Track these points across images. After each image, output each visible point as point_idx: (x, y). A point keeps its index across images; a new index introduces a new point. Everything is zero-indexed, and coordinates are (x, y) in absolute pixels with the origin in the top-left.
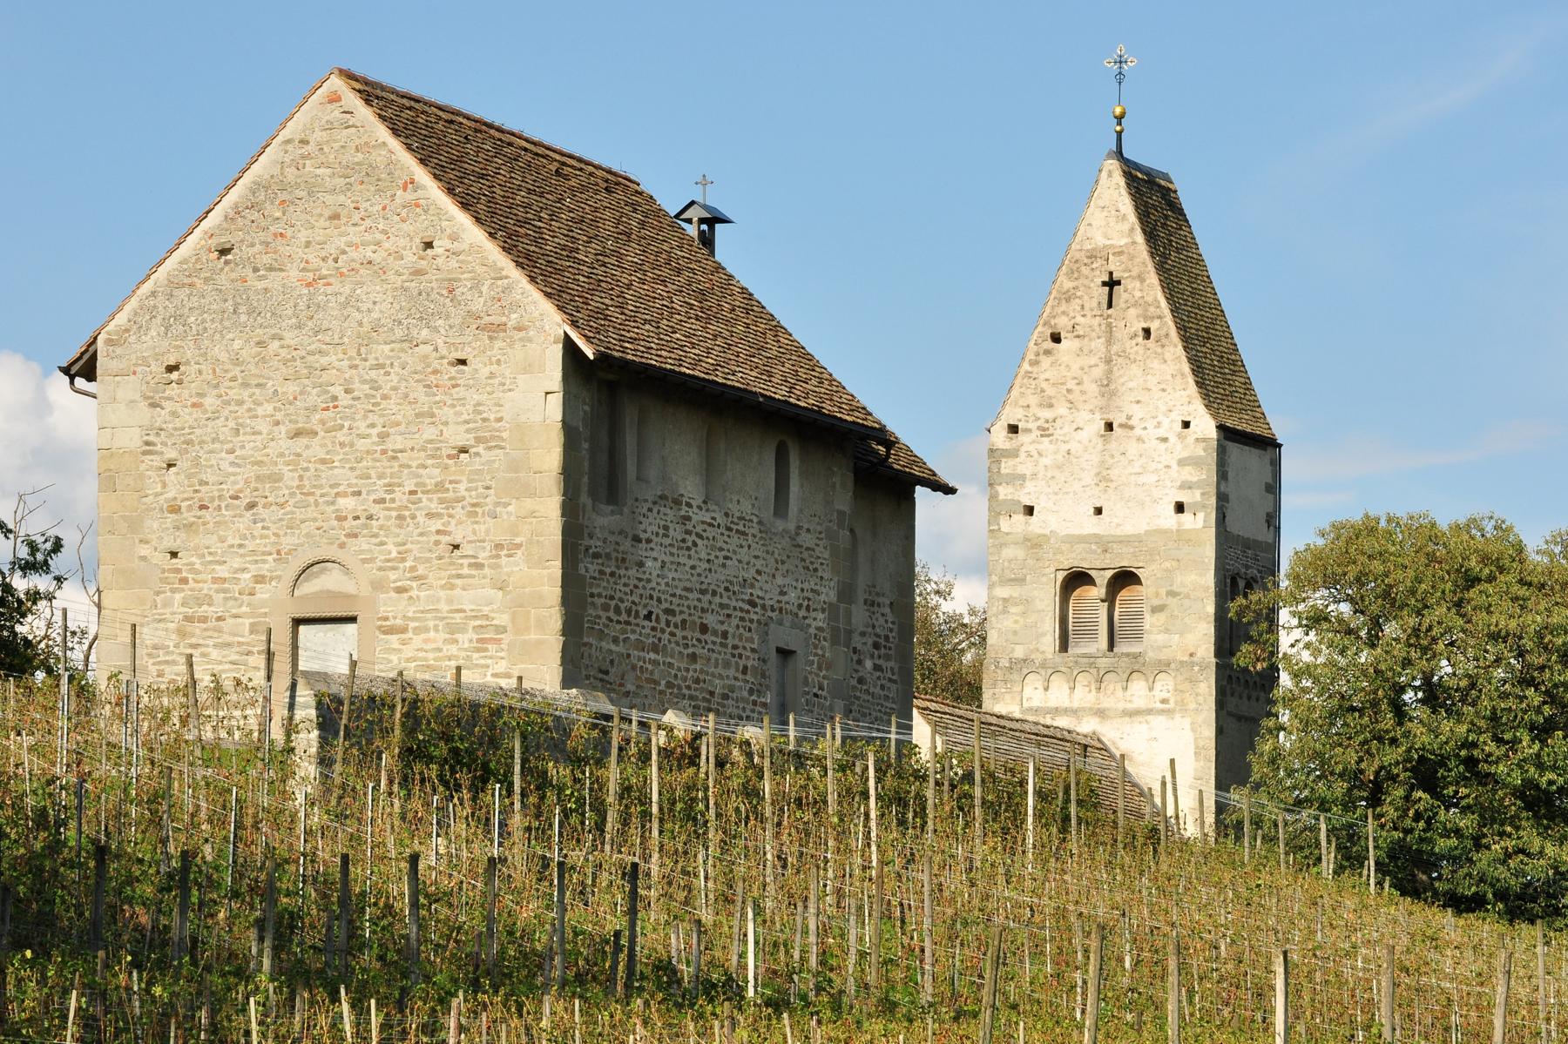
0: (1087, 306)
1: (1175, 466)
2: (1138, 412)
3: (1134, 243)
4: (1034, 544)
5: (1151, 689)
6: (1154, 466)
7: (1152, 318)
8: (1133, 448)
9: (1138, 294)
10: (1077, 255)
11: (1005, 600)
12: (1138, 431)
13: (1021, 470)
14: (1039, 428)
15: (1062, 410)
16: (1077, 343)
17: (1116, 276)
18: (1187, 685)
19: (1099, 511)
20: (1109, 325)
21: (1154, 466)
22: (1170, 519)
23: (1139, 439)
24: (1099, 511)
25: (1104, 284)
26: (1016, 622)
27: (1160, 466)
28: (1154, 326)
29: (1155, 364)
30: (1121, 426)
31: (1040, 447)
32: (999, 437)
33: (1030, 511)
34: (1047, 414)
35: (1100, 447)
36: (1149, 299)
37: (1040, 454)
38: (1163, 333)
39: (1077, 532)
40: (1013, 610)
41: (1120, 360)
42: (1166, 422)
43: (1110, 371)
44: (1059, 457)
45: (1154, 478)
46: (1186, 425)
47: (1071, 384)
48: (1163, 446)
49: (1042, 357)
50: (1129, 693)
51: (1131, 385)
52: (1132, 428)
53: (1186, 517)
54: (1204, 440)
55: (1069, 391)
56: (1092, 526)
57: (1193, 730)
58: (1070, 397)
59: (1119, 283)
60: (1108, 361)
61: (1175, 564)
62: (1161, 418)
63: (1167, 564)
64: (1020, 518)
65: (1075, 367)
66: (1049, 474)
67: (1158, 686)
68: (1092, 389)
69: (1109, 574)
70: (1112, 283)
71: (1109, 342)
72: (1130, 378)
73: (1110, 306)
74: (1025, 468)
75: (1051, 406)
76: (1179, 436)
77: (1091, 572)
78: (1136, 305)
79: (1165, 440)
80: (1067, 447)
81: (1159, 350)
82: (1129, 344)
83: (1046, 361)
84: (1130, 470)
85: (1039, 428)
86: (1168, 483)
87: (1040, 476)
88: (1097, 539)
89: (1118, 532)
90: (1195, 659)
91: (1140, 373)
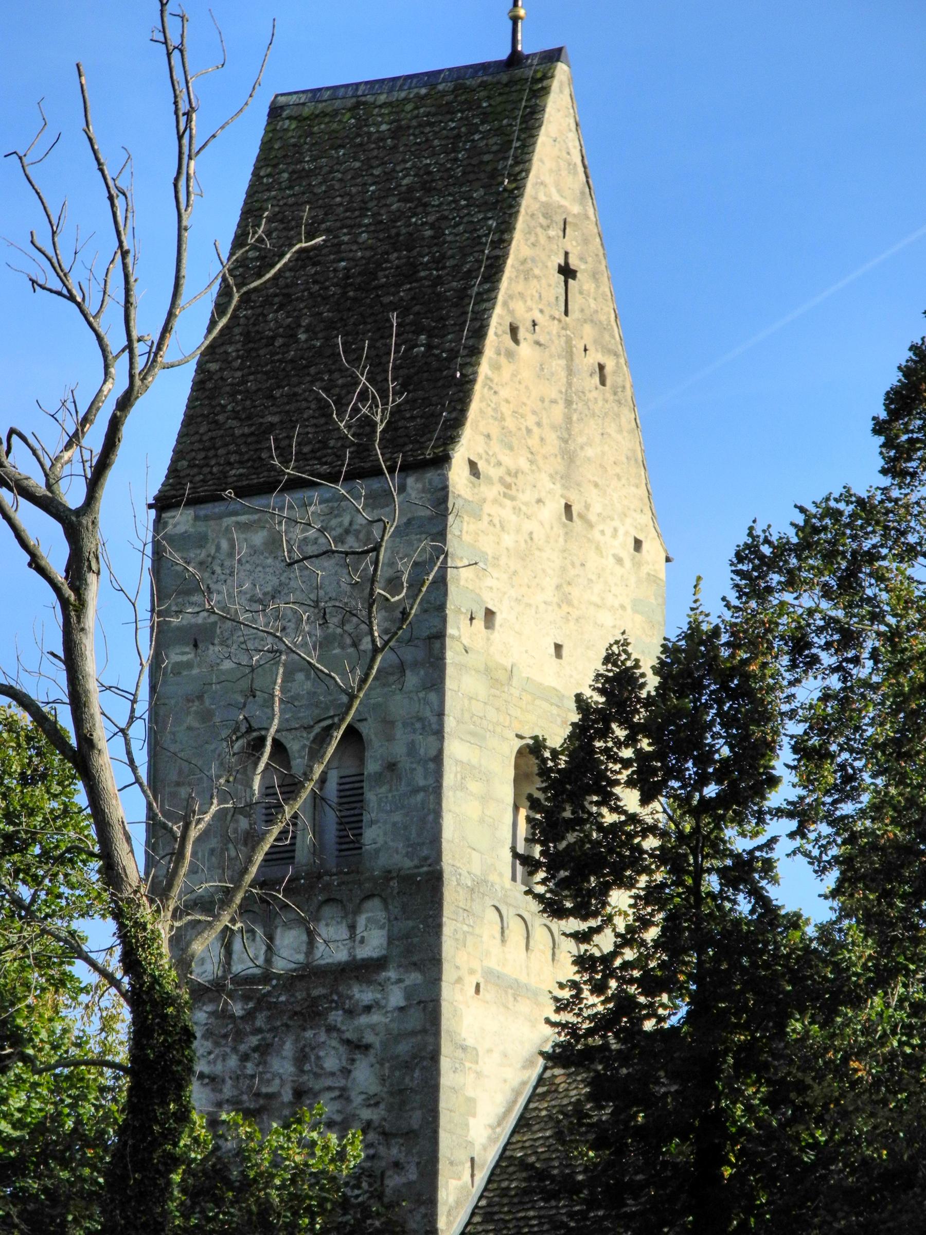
3: (587, 218)
17: (574, 262)
20: (569, 341)
29: (612, 429)
36: (603, 318)
60: (569, 403)
70: (567, 272)
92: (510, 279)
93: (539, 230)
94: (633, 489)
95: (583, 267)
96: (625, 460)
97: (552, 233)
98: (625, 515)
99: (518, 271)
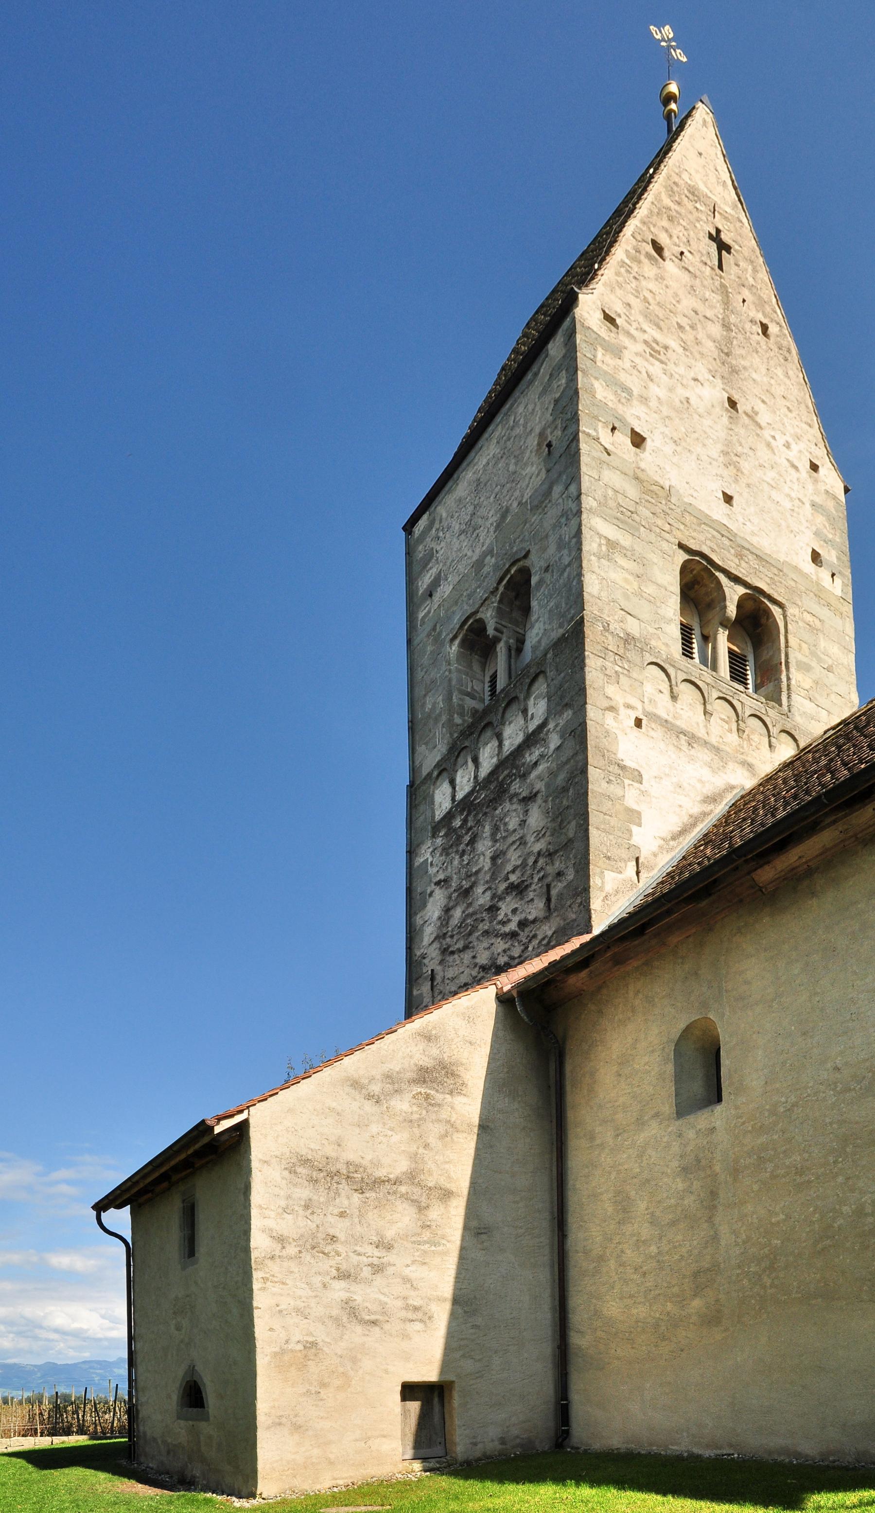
8: (763, 453)
11: (612, 545)
14: (646, 342)
17: (725, 237)
21: (787, 490)
26: (626, 580)
29: (779, 372)
31: (651, 369)
35: (725, 420)
40: (622, 561)
41: (740, 336)
47: (684, 322)
52: (761, 428)
55: (680, 327)
60: (726, 326)
64: (623, 440)
66: (665, 411)
71: (727, 303)
73: (720, 267)
82: (748, 326)
85: (646, 342)
95: (737, 247)
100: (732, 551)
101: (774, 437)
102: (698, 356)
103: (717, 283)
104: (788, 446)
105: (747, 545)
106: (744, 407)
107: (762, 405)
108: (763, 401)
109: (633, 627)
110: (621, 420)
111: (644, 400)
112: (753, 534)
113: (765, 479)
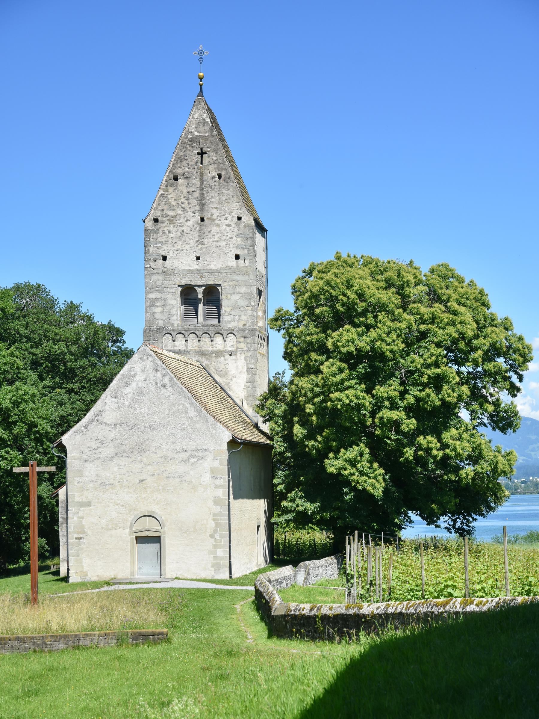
0: (190, 164)
1: (235, 238)
2: (216, 213)
4: (167, 273)
5: (225, 341)
6: (225, 237)
7: (222, 169)
8: (214, 230)
9: (215, 158)
10: (185, 140)
12: (217, 222)
13: (160, 239)
14: (169, 220)
15: (179, 212)
16: (186, 181)
18: (242, 339)
19: (198, 258)
20: (202, 174)
21: (225, 237)
22: (233, 262)
23: (218, 225)
24: (198, 258)
25: (198, 153)
27: (228, 238)
28: (223, 173)
30: (207, 219)
31: (169, 229)
32: (150, 224)
33: (164, 258)
34: (172, 213)
37: (169, 232)
38: (228, 176)
39: (187, 268)
42: (230, 217)
43: (202, 194)
44: (179, 234)
45: (224, 243)
46: (239, 219)
48: (228, 228)
49: (169, 187)
50: (214, 343)
51: (213, 200)
52: (214, 220)
53: (241, 261)
54: (249, 226)
55: (182, 203)
56: (195, 266)
57: (246, 360)
58: (183, 205)
59: (205, 153)
60: (202, 189)
61: (236, 283)
62: (227, 215)
63: (231, 283)
65: (185, 191)
66: (174, 242)
67: (228, 340)
68: (194, 202)
69: (203, 288)
70: (202, 153)
72: (212, 197)
73: (202, 163)
74: (162, 239)
75: (174, 210)
76: (236, 223)
77: (196, 288)
78: (214, 163)
79: (229, 226)
80: (182, 228)
81: (226, 184)
83: (171, 190)
84: (213, 239)
86: (232, 246)
87: (170, 242)
88: (198, 271)
89: (208, 268)
90: (246, 327)
91: (217, 195)
92: (173, 164)
93: (188, 146)
94: (237, 204)
95: (209, 149)
96: (231, 196)
97: (193, 145)
98: (232, 212)
99: (177, 161)
100: (199, 277)
101: (220, 220)
102: (188, 210)
103: (198, 173)
104: (226, 219)
105: (205, 271)
106: (208, 217)
107: (215, 210)
108: (216, 208)
109: (161, 324)
110: (158, 255)
111: (166, 242)
112: (208, 265)
113: (216, 239)
